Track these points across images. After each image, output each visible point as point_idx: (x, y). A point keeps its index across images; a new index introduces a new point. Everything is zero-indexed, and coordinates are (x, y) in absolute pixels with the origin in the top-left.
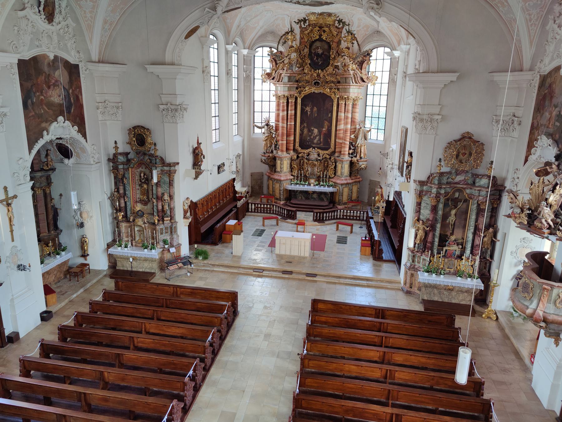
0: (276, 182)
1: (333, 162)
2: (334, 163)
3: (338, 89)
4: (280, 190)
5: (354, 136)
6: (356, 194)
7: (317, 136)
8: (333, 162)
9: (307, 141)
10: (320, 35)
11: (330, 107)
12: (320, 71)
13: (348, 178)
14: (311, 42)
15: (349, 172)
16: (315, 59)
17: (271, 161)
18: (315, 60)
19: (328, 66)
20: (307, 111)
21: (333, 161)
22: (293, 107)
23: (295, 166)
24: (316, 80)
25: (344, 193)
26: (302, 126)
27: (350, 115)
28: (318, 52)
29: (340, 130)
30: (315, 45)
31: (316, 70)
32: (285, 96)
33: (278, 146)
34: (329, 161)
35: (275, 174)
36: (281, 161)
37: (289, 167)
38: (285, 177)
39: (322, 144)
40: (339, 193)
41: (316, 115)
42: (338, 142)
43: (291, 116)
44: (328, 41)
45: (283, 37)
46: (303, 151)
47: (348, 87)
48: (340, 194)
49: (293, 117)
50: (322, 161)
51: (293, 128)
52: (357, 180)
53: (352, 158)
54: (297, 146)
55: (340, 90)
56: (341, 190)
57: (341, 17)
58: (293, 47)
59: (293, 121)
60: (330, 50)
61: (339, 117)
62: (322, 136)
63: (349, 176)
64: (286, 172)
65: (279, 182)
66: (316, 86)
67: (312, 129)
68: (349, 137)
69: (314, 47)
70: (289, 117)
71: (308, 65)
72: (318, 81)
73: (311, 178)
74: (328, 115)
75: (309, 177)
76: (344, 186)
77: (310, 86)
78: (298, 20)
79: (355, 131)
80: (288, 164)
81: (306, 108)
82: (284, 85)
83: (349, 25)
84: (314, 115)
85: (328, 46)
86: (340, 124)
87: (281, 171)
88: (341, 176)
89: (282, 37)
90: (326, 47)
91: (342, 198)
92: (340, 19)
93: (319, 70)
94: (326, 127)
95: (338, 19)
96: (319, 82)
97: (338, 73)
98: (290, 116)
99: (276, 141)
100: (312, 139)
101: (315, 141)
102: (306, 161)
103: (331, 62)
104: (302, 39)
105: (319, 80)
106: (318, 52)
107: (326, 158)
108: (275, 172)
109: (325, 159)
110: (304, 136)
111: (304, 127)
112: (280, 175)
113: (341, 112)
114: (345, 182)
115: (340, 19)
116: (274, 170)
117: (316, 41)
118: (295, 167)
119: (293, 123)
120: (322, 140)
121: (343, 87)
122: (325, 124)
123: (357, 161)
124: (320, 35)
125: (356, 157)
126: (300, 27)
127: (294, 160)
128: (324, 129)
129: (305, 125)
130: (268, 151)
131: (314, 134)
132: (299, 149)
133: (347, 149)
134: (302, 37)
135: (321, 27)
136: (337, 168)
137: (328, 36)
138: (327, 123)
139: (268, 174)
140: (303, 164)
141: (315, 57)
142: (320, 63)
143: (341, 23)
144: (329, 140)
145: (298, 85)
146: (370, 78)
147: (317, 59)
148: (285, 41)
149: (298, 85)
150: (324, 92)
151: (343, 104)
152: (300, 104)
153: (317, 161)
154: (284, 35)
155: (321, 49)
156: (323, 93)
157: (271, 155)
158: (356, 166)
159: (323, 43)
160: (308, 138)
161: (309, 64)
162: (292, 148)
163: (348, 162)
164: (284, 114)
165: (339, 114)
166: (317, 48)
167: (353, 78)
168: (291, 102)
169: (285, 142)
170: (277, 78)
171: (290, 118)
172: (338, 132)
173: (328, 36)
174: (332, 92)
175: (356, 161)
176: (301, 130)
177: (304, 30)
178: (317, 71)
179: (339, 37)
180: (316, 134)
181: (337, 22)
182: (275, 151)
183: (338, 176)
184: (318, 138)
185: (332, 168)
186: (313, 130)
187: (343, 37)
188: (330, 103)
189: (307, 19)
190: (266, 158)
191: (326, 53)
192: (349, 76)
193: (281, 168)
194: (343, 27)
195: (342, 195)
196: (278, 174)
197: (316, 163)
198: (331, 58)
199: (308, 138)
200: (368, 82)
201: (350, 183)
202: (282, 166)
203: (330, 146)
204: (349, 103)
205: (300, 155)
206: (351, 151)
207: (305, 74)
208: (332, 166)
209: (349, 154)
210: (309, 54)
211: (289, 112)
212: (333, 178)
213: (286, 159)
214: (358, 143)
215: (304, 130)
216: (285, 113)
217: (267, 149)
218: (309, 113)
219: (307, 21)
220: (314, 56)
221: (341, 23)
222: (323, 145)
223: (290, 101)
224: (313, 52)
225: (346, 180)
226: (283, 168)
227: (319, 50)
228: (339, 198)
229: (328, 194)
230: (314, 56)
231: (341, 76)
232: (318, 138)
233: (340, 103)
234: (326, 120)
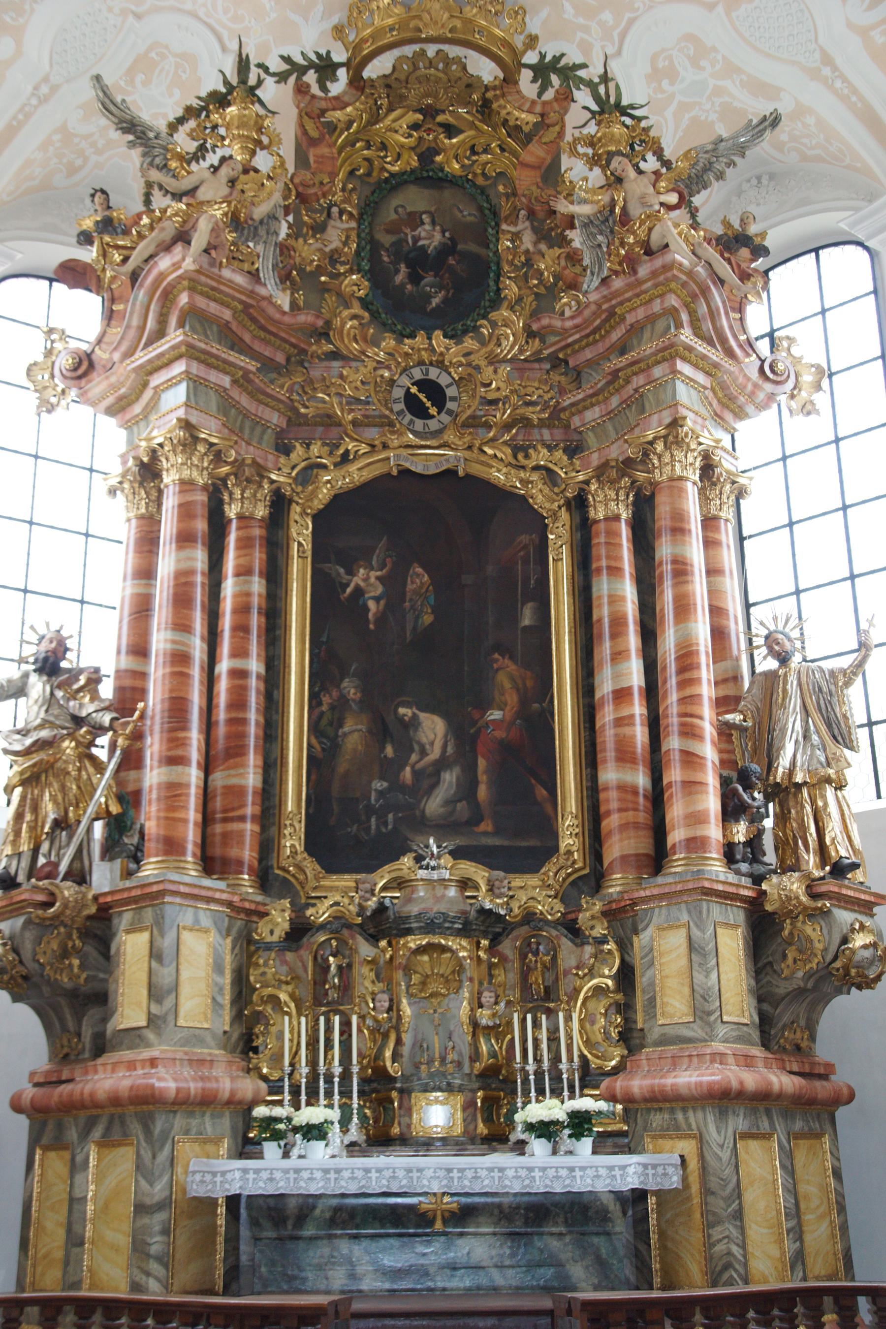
0: (106, 1144)
1: (603, 941)
2: (611, 946)
3: (574, 450)
4: (141, 1209)
5: (745, 721)
6: (824, 1227)
7: (441, 764)
8: (603, 941)
9: (370, 810)
10: (427, 155)
11: (526, 562)
12: (438, 333)
13: (757, 1052)
14: (367, 191)
15: (754, 1002)
16: (399, 278)
17: (65, 953)
18: (402, 285)
19: (497, 302)
20: (359, 592)
21: (600, 930)
22: (258, 557)
23: (283, 997)
24: (421, 363)
25: (749, 1196)
26: (326, 700)
27: (696, 554)
28: (416, 239)
29: (622, 695)
30: (395, 202)
31: (412, 336)
32: (196, 439)
33: (131, 840)
34: (566, 944)
35: (100, 1061)
36: (159, 925)
37: (226, 999)
38: (187, 1072)
39: (486, 826)
40: (706, 1191)
41: (428, 619)
42: (622, 788)
43: (242, 609)
44: (480, 181)
45: (192, 124)
46: (346, 881)
47: (657, 372)
48: (717, 1205)
49: (255, 621)
50: (507, 947)
51: (253, 699)
52: (821, 1088)
53: (758, 880)
54: (294, 853)
55: (591, 439)
56: (725, 1155)
57: (550, 50)
58: (256, 171)
59: (254, 647)
60: (498, 225)
61: (603, 612)
62: (482, 763)
63: (756, 1035)
64: (195, 1037)
65: (136, 1128)
66: (419, 424)
67: (400, 720)
68: (707, 711)
69: (389, 213)
70: (227, 622)
71: (357, 309)
72: (433, 373)
73: (426, 1089)
74: (515, 619)
75: (405, 1078)
76: (739, 1122)
77: (372, 433)
78: (287, 59)
79: (737, 699)
80: (218, 968)
81: (351, 572)
82: (196, 368)
83: (605, 78)
84: (410, 617)
85: (481, 209)
86: (619, 656)
87: (152, 1020)
88: (696, 1031)
89: (181, 121)
90: (467, 214)
91: (743, 1246)
92: (543, 56)
93: (430, 338)
94: (512, 699)
95: (531, 58)
96: (444, 380)
97: (565, 333)
98: (235, 611)
99: (120, 799)
100: (402, 788)
101: (434, 805)
102: (365, 950)
103: (511, 289)
104: (314, 142)
105: (440, 364)
106: (416, 239)
107: (529, 918)
108: (101, 1047)
109: (524, 930)
110: (342, 766)
111: (341, 706)
112: (146, 1054)
113: (615, 571)
114: (750, 1080)
115: (543, 56)
116: (87, 1033)
117: (397, 183)
118: (274, 1000)
119: (255, 665)
120: (483, 792)
121: (615, 401)
122: (502, 679)
123: (814, 896)
124: (427, 155)
125: (785, 868)
126: (301, 89)
127: (268, 947)
128: (495, 715)
129: (350, 688)
130: (42, 861)
131: (423, 753)
132: (311, 866)
133: (712, 803)
134: (314, 134)
135: (429, 112)
136: (641, 981)
137: (473, 152)
138: (512, 667)
139: (29, 1092)
140: (346, 988)
141: (403, 268)
142: (435, 302)
143: (555, 79)
144: (541, 793)
145: (295, 420)
146: (780, 367)
147: (415, 278)
148: (202, 148)
149: (295, 420)
150: (477, 470)
151: (617, 518)
152: (308, 546)
153: (465, 931)
154: (190, 112)
155: (433, 223)
156: (468, 476)
157: (68, 890)
158: (805, 948)
159: (447, 193)
160: (379, 785)
161: (365, 303)
162: (248, 853)
163: (737, 915)
164: (184, 566)
165: (602, 587)
166: (414, 220)
167: (684, 317)
168: (241, 517)
169: (194, 775)
170: (142, 328)
171: (235, 629)
172: (607, 716)
173: (473, 152)
174: (532, 463)
175: (804, 899)
176: (315, 728)
177: (323, 105)
178: (420, 340)
179: (550, 135)
180: (435, 754)
181: (526, 75)
182: (106, 865)
183: (665, 1041)
184: (450, 778)
185: (598, 991)
186: (415, 722)
187: (576, 140)
188: (524, 539)
189: (339, 56)
190: (20, 921)
191: (473, 247)
192: (656, 307)
193: (155, 993)
194: (565, 98)
195: (739, 1215)
196: (127, 1055)
197: (461, 947)
198: (506, 268)
199: (379, 785)
200: (768, 387)
201: (780, 1096)
202: (165, 974)
203: (554, 836)
204: (678, 471)
205: (321, 913)
206: (741, 832)
207: (336, 364)
208: (591, 974)
209: (730, 854)
210: (358, 253)
211: (229, 587)
212: (616, 1071)
213: (205, 920)
214: (784, 762)
215: (341, 725)
216: (199, 558)
217: (35, 851)
218: (372, 605)
219: (342, 73)
220: (395, 263)
221: (555, 79)
222: (497, 832)
223: (232, 511)
224: (387, 240)
225: (748, 1061)
226: (175, 988)
227: (422, 231)
228: (709, 1244)
229: (604, 1216)
230: (395, 263)
231: (588, 354)
232: (450, 778)
233: (598, 513)
234: (507, 651)
